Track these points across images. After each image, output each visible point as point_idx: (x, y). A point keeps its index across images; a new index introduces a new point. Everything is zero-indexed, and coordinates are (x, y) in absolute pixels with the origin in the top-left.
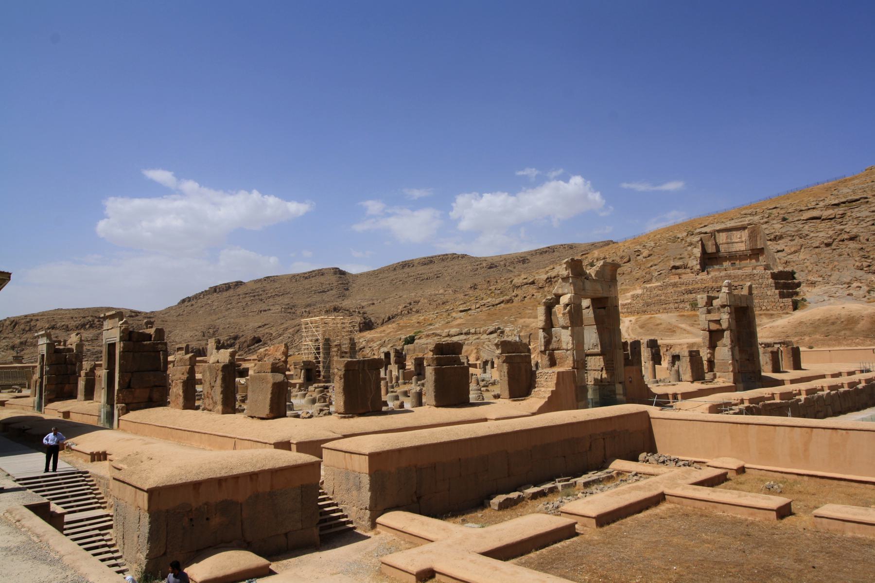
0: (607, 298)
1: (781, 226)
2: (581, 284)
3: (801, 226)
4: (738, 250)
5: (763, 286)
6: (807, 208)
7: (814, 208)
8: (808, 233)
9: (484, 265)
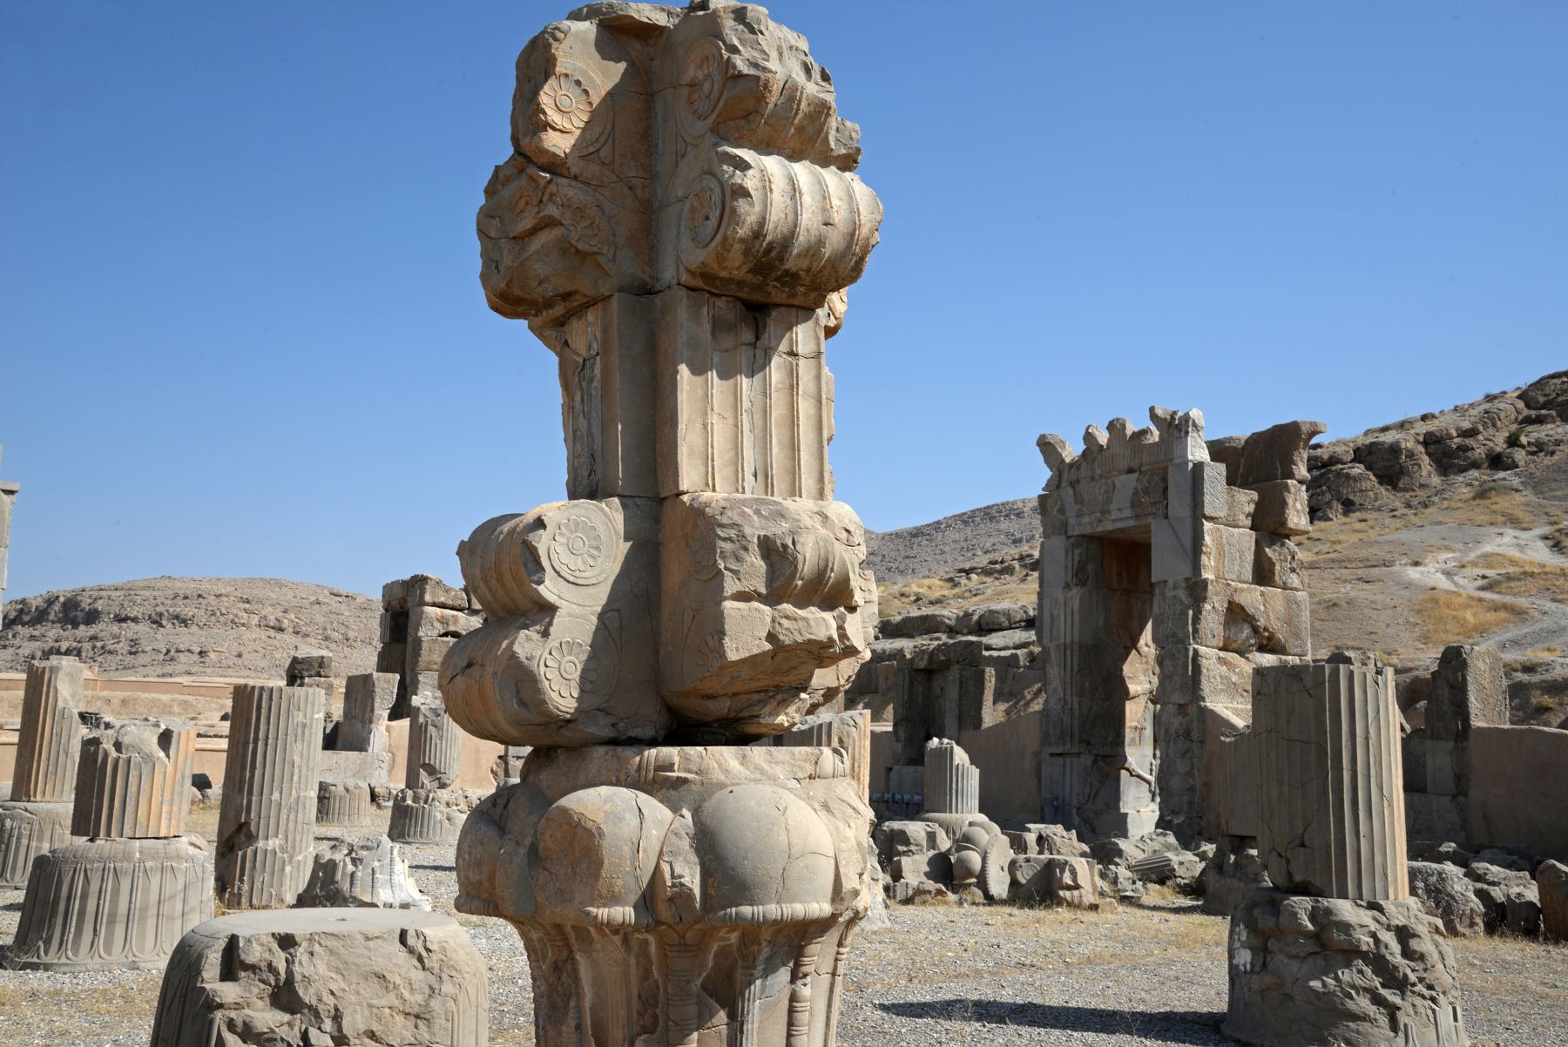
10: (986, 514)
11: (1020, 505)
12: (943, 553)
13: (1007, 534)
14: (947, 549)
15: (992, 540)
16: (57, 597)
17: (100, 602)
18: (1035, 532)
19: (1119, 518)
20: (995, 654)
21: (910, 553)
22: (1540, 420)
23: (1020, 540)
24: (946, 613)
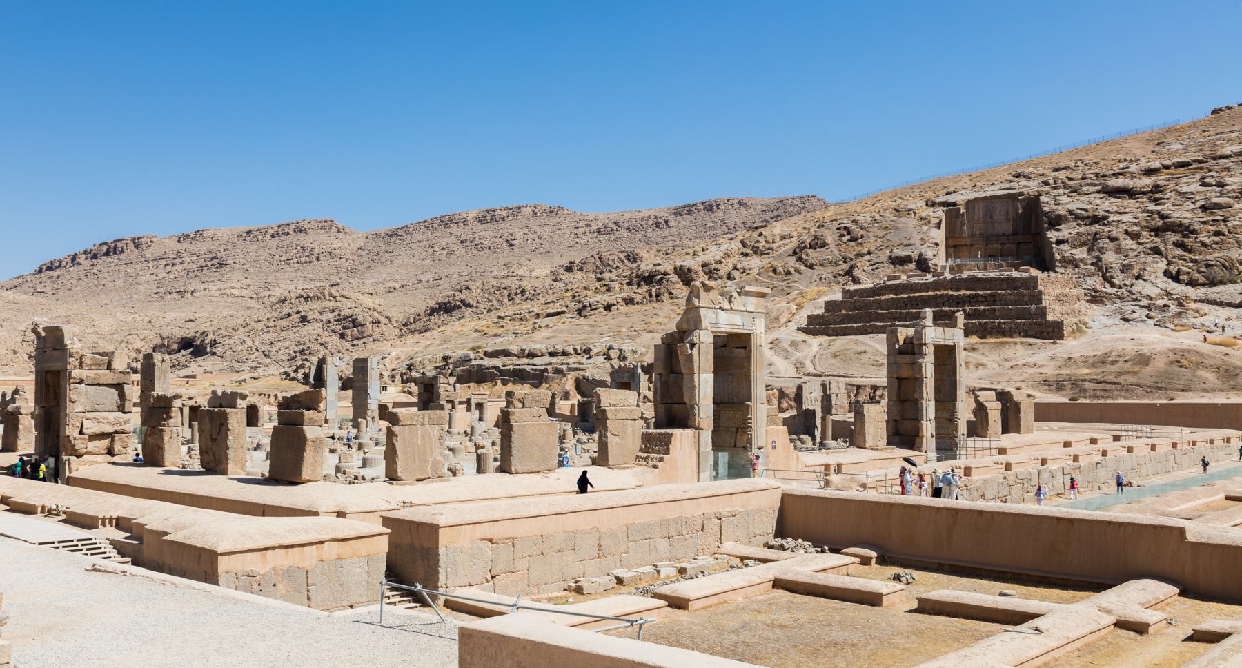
0: (750, 335)
1: (1069, 199)
2: (714, 316)
3: (1098, 201)
4: (1001, 232)
5: (1026, 299)
6: (1112, 172)
7: (1121, 174)
8: (1107, 214)
9: (594, 228)
11: (465, 215)
13: (457, 237)
14: (415, 246)
15: (446, 240)
18: (475, 235)
19: (626, 380)
20: (538, 368)
22: (747, 255)
24: (512, 348)
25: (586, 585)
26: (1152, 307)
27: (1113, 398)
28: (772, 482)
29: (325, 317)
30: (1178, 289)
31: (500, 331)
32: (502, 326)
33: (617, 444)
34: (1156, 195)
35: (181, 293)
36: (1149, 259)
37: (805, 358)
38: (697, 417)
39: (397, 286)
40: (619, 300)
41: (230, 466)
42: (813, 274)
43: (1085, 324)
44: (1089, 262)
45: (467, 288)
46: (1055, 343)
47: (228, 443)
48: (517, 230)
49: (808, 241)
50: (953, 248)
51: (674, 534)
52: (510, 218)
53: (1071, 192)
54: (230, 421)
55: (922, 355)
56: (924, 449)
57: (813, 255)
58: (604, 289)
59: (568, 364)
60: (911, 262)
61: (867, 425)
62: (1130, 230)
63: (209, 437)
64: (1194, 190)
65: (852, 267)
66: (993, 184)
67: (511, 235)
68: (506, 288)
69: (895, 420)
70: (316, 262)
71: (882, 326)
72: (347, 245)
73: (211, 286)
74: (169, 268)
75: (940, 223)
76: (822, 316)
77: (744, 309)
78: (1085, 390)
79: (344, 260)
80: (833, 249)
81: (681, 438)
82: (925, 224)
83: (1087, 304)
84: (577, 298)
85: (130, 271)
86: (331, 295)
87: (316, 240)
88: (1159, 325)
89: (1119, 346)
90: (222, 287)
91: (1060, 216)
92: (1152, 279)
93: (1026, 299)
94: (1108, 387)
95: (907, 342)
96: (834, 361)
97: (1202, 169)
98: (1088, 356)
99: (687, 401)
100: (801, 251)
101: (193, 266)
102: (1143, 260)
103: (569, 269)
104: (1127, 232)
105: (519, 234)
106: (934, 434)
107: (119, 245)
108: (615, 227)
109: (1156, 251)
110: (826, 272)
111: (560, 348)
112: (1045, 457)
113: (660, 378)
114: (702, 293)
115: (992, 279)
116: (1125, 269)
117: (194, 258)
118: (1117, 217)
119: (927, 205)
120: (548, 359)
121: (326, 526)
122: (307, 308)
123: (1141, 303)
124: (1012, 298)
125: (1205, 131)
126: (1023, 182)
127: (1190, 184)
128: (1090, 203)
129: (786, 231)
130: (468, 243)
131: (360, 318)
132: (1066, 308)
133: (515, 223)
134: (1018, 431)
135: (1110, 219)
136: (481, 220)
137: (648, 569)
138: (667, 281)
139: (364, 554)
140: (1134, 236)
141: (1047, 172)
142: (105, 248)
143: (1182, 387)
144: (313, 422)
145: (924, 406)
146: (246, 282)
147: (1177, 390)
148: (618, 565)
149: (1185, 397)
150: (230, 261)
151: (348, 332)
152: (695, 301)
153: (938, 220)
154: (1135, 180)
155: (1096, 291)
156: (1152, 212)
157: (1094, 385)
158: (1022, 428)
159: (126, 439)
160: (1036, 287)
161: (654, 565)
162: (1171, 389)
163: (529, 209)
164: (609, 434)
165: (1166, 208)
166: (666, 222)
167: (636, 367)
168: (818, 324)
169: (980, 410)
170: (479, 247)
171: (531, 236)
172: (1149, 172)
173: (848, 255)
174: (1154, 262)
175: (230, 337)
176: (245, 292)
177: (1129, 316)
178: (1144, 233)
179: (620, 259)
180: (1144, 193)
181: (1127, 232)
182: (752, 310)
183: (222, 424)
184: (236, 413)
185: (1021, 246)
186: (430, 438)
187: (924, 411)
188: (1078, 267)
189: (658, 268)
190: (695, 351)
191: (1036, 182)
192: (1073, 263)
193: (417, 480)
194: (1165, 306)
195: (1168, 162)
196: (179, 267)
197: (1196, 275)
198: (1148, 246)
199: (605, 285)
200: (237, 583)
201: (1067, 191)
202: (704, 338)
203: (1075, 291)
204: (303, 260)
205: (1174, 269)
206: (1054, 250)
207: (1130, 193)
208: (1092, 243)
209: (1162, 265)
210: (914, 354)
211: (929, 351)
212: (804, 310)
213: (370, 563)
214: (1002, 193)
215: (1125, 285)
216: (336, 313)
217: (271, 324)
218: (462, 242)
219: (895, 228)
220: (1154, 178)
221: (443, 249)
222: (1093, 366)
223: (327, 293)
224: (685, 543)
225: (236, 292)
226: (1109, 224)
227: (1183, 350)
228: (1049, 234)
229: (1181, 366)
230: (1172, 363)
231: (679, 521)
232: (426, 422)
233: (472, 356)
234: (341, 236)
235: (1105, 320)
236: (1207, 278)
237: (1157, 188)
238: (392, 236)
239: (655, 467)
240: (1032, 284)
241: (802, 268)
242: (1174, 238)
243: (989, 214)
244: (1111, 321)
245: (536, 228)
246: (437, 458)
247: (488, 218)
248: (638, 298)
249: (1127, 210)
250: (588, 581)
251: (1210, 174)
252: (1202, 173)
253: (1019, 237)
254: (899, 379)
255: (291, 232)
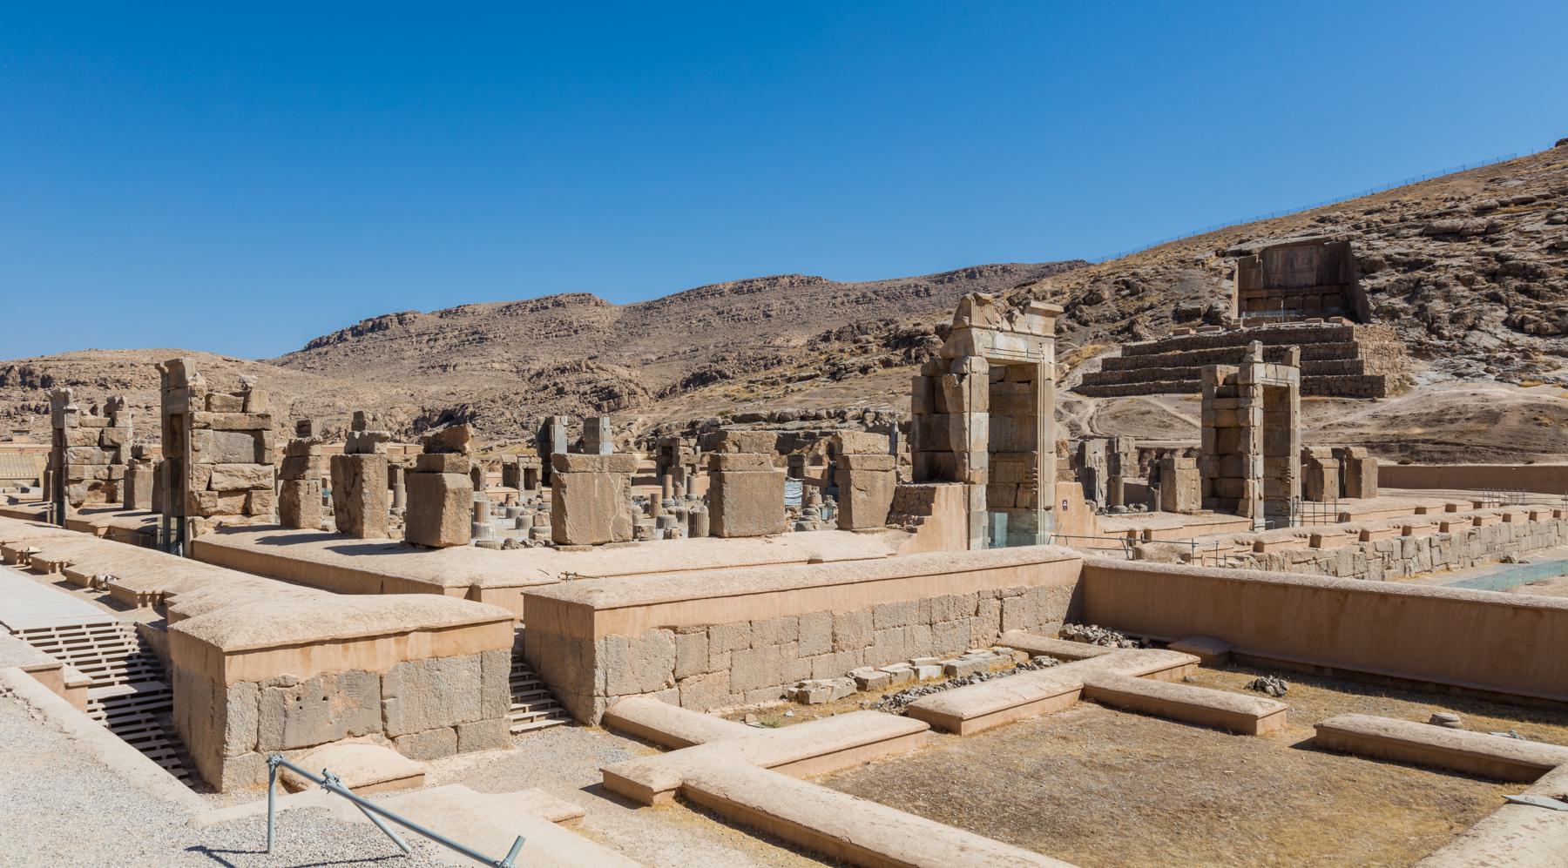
0: (1035, 365)
1: (1386, 243)
2: (990, 339)
3: (1421, 245)
4: (1302, 283)
6: (1437, 212)
8: (1432, 258)
9: (853, 297)
10: (699, 293)
11: (721, 287)
12: (669, 321)
14: (671, 318)
15: (703, 312)
16: (12, 367)
17: (51, 370)
21: (647, 322)
23: (723, 312)
24: (762, 412)
25: (813, 691)
26: (1492, 361)
27: (1454, 461)
28: (1079, 554)
29: (581, 390)
30: (1521, 339)
31: (750, 396)
32: (753, 391)
33: (864, 501)
34: (1493, 236)
35: (444, 368)
36: (1486, 307)
37: (1081, 420)
38: (967, 468)
39: (654, 358)
40: (877, 362)
41: (366, 527)
42: (1087, 331)
43: (1409, 379)
44: (1411, 312)
45: (723, 359)
46: (1373, 401)
47: (363, 497)
48: (774, 301)
49: (1082, 296)
50: (1248, 302)
51: (938, 620)
52: (767, 289)
53: (1388, 236)
54: (365, 470)
55: (1250, 397)
56: (1250, 513)
57: (1088, 312)
58: (859, 351)
59: (821, 428)
60: (1199, 316)
61: (1178, 483)
62: (1461, 275)
63: (342, 490)
64: (1539, 229)
65: (1133, 323)
66: (1293, 231)
67: (768, 305)
68: (762, 359)
69: (1212, 479)
70: (574, 336)
71: (1168, 385)
72: (603, 319)
73: (473, 361)
74: (432, 343)
75: (1233, 272)
76: (1099, 375)
77: (1028, 331)
78: (1418, 453)
79: (601, 333)
80: (1110, 304)
81: (947, 496)
82: (1216, 275)
83: (1410, 359)
84: (832, 361)
85: (395, 346)
86: (588, 367)
87: (576, 314)
88: (1501, 381)
89: (1460, 402)
90: (483, 361)
91: (1375, 262)
92: (1491, 329)
93: (1338, 352)
94: (1448, 448)
95: (1229, 381)
96: (1114, 423)
97: (1548, 205)
98: (1421, 414)
99: (954, 446)
100: (1074, 307)
101: (455, 341)
102: (1480, 307)
103: (826, 339)
104: (1457, 277)
105: (776, 305)
106: (1262, 496)
107: (384, 321)
108: (874, 297)
109: (1494, 298)
110: (1103, 329)
111: (812, 412)
112: (1407, 524)
113: (920, 419)
114: (975, 309)
115: (1297, 330)
116: (1455, 319)
117: (456, 333)
118: (1445, 262)
119: (1217, 255)
120: (798, 424)
121: (452, 608)
122: (564, 380)
123: (1478, 356)
124: (1321, 351)
125: (1549, 165)
126: (1329, 227)
127: (1534, 222)
128: (1412, 247)
129: (1058, 286)
130: (725, 314)
131: (617, 390)
132: (1386, 363)
133: (771, 294)
134: (1358, 495)
135: (1437, 264)
136: (738, 291)
137: (902, 667)
138: (928, 341)
139: (474, 651)
140: (1468, 282)
141: (1357, 216)
142: (371, 323)
143: (1543, 448)
144: (455, 469)
145: (1251, 460)
146: (507, 356)
147: (1537, 451)
148: (861, 661)
149: (1548, 460)
150: (491, 336)
151: (605, 403)
152: (966, 320)
153: (1229, 271)
154: (1466, 220)
155: (1420, 343)
156: (1488, 254)
157: (1430, 447)
158: (1363, 492)
159: (265, 496)
160: (1350, 339)
161: (910, 662)
162: (1529, 451)
163: (786, 280)
164: (852, 488)
165: (1506, 249)
166: (927, 290)
167: (892, 425)
168: (1096, 384)
169: (1313, 468)
170: (736, 319)
171: (788, 307)
172: (1482, 211)
173: (1126, 310)
174: (1492, 310)
175: (490, 409)
176: (506, 366)
177: (1463, 371)
178: (1479, 278)
179: (878, 327)
180: (1478, 234)
181: (1457, 277)
182: (1039, 333)
183: (356, 474)
184: (373, 460)
185: (1327, 298)
186: (612, 490)
187: (1251, 468)
188: (1399, 318)
189: (919, 328)
190: (965, 384)
191: (1346, 226)
192: (1392, 314)
193: (594, 545)
194: (1508, 358)
195: (1506, 199)
196: (441, 342)
197: (1546, 324)
198: (1484, 292)
199: (861, 347)
200: (259, 697)
201: (1382, 235)
202: (978, 367)
203: (1395, 344)
204: (562, 333)
205: (1516, 316)
206: (1369, 300)
207: (1459, 235)
208: (1413, 292)
209: (1502, 313)
210: (1238, 397)
211: (1259, 392)
212: (1078, 369)
213: (486, 662)
214: (1304, 239)
215: (1456, 336)
216: (593, 385)
217: (529, 396)
218: (719, 314)
219: (1181, 280)
220: (1489, 217)
221: (700, 321)
222: (1426, 424)
223: (583, 364)
224: (952, 632)
225: (496, 366)
226: (1435, 269)
227: (1541, 406)
228: (1362, 283)
229: (1540, 425)
230: (1527, 421)
231: (945, 602)
232: (606, 469)
233: (720, 420)
234: (599, 309)
235: (1433, 375)
236: (1559, 327)
237: (1493, 228)
238: (648, 309)
239: (912, 531)
240: (1346, 336)
241: (1076, 325)
242: (1517, 283)
243: (1289, 262)
244: (1441, 377)
245: (794, 299)
246: (621, 516)
247: (745, 289)
248: (897, 359)
249: (1457, 253)
250: (817, 685)
251: (1560, 210)
252: (1549, 209)
253: (1325, 287)
254: (1218, 429)
255: (550, 306)
